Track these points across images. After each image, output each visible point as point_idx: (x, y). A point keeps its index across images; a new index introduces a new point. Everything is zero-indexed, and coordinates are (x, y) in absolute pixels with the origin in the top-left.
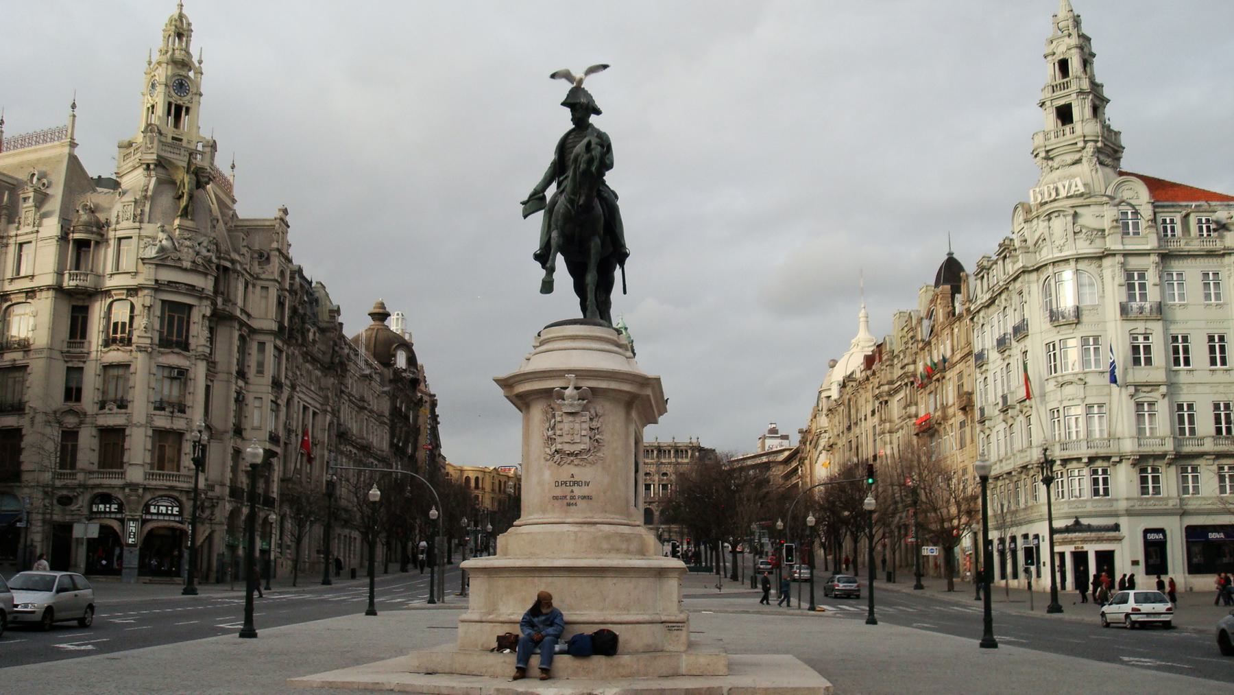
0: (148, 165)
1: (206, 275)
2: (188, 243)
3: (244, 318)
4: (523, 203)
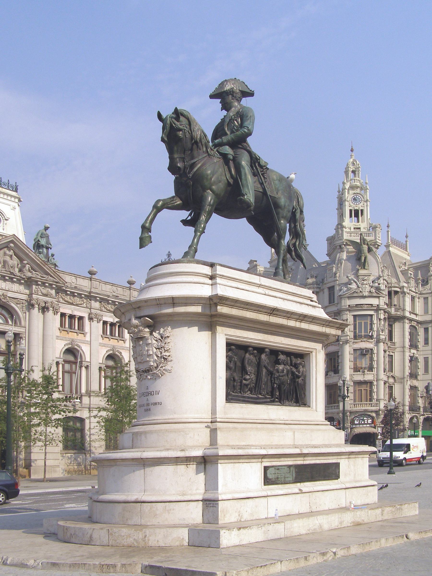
0: (340, 246)
1: (379, 297)
2: (365, 282)
3: (413, 316)
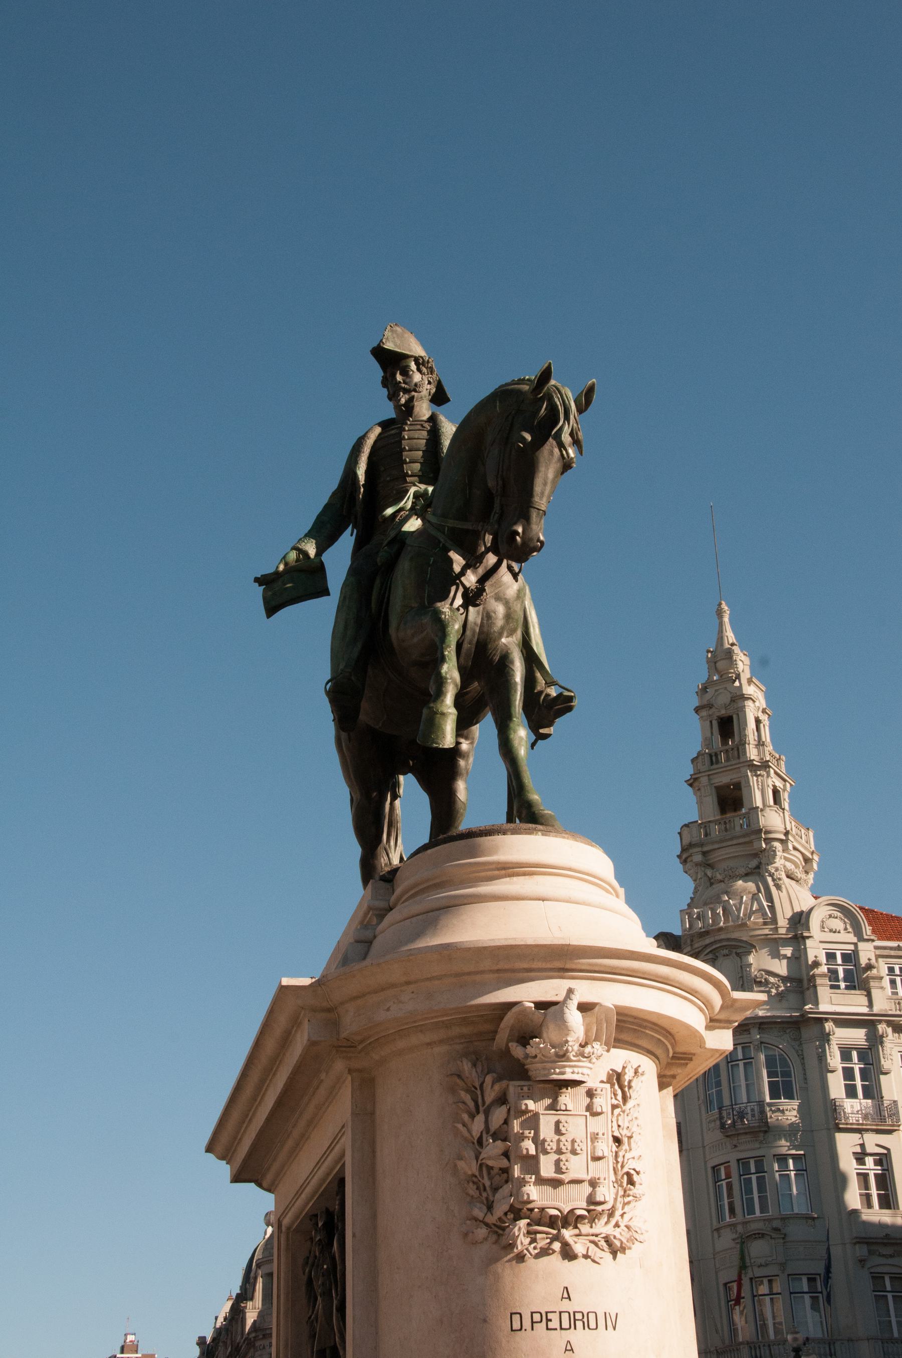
4: (259, 581)
